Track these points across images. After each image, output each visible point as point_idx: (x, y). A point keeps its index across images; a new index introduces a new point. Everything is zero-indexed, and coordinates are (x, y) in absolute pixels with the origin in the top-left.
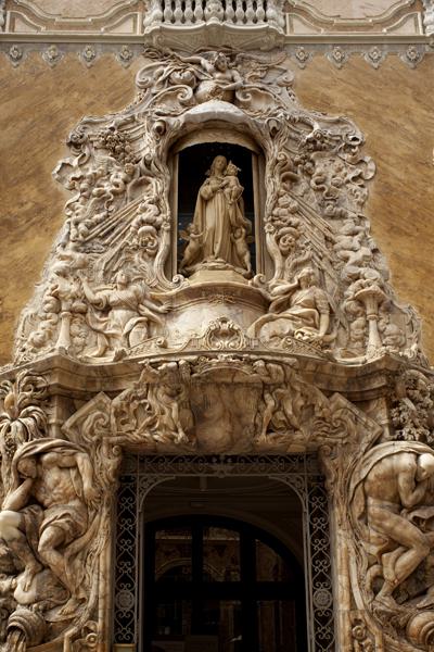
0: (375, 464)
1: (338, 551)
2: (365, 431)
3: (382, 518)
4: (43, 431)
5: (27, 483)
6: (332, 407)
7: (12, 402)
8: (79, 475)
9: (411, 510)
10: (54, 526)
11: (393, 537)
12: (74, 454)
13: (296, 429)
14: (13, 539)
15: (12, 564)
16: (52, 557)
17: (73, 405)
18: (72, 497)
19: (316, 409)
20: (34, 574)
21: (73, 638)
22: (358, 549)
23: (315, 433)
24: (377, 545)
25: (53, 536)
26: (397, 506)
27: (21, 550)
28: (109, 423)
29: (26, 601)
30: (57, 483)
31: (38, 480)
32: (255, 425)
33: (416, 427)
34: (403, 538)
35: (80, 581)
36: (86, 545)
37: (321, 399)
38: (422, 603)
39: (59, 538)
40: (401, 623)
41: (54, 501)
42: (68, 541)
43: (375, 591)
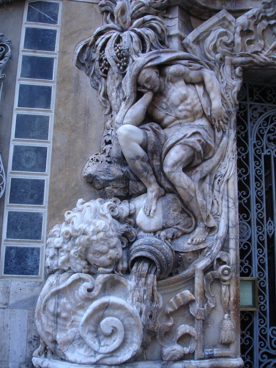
4: (162, 43)
5: (147, 97)
7: (123, 11)
8: (206, 93)
10: (185, 144)
12: (201, 68)
14: (138, 157)
15: (127, 187)
16: (182, 179)
17: (189, 21)
18: (199, 115)
20: (159, 197)
21: (206, 270)
25: (183, 156)
27: (145, 169)
28: (233, 42)
29: (153, 227)
30: (184, 99)
31: (159, 94)
35: (209, 207)
36: (214, 168)
39: (188, 159)
41: (177, 118)
42: (197, 161)
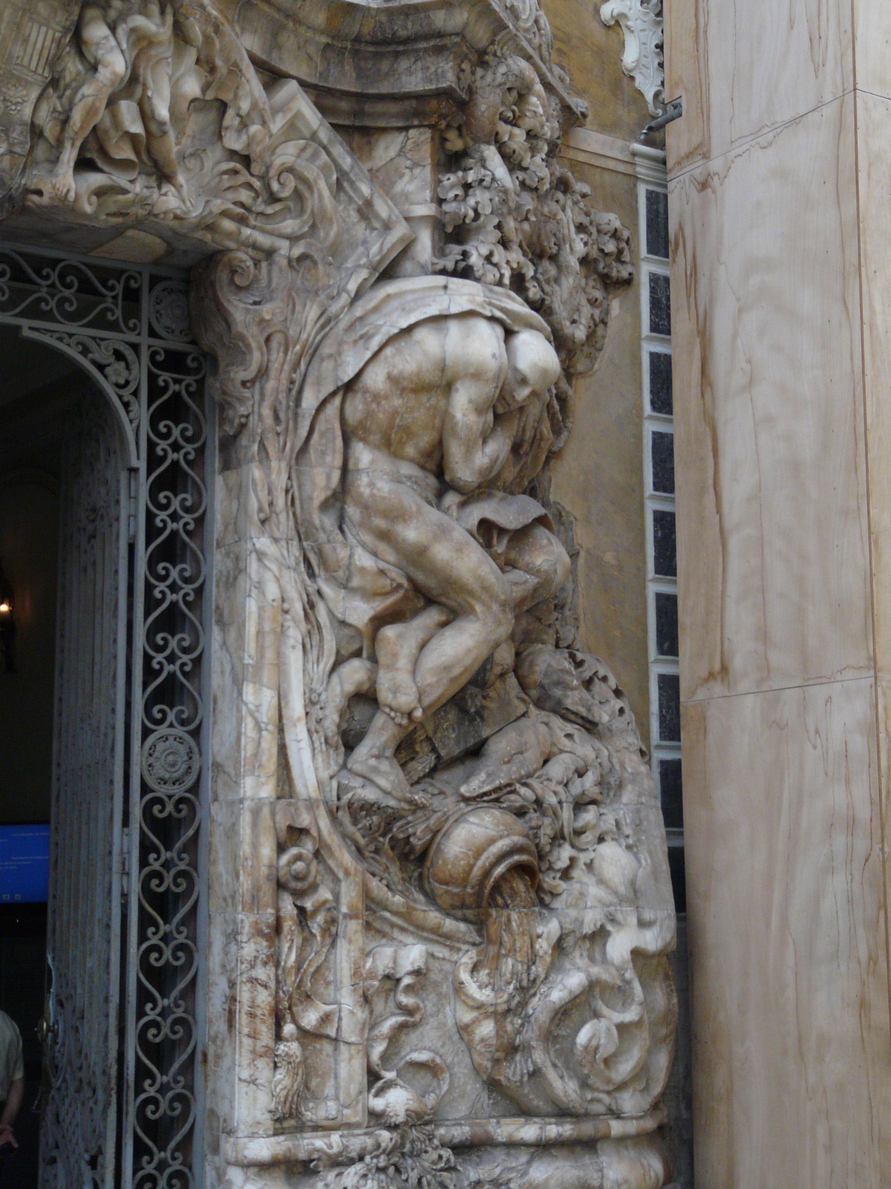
0: (390, 341)
1: (252, 606)
2: (360, 230)
3: (397, 515)
6: (277, 125)
9: (471, 495)
11: (420, 577)
13: (162, 175)
22: (312, 606)
23: (218, 205)
24: (370, 595)
26: (432, 481)
32: (35, 132)
33: (504, 243)
34: (451, 584)
38: (476, 784)
40: (417, 843)
43: (349, 740)
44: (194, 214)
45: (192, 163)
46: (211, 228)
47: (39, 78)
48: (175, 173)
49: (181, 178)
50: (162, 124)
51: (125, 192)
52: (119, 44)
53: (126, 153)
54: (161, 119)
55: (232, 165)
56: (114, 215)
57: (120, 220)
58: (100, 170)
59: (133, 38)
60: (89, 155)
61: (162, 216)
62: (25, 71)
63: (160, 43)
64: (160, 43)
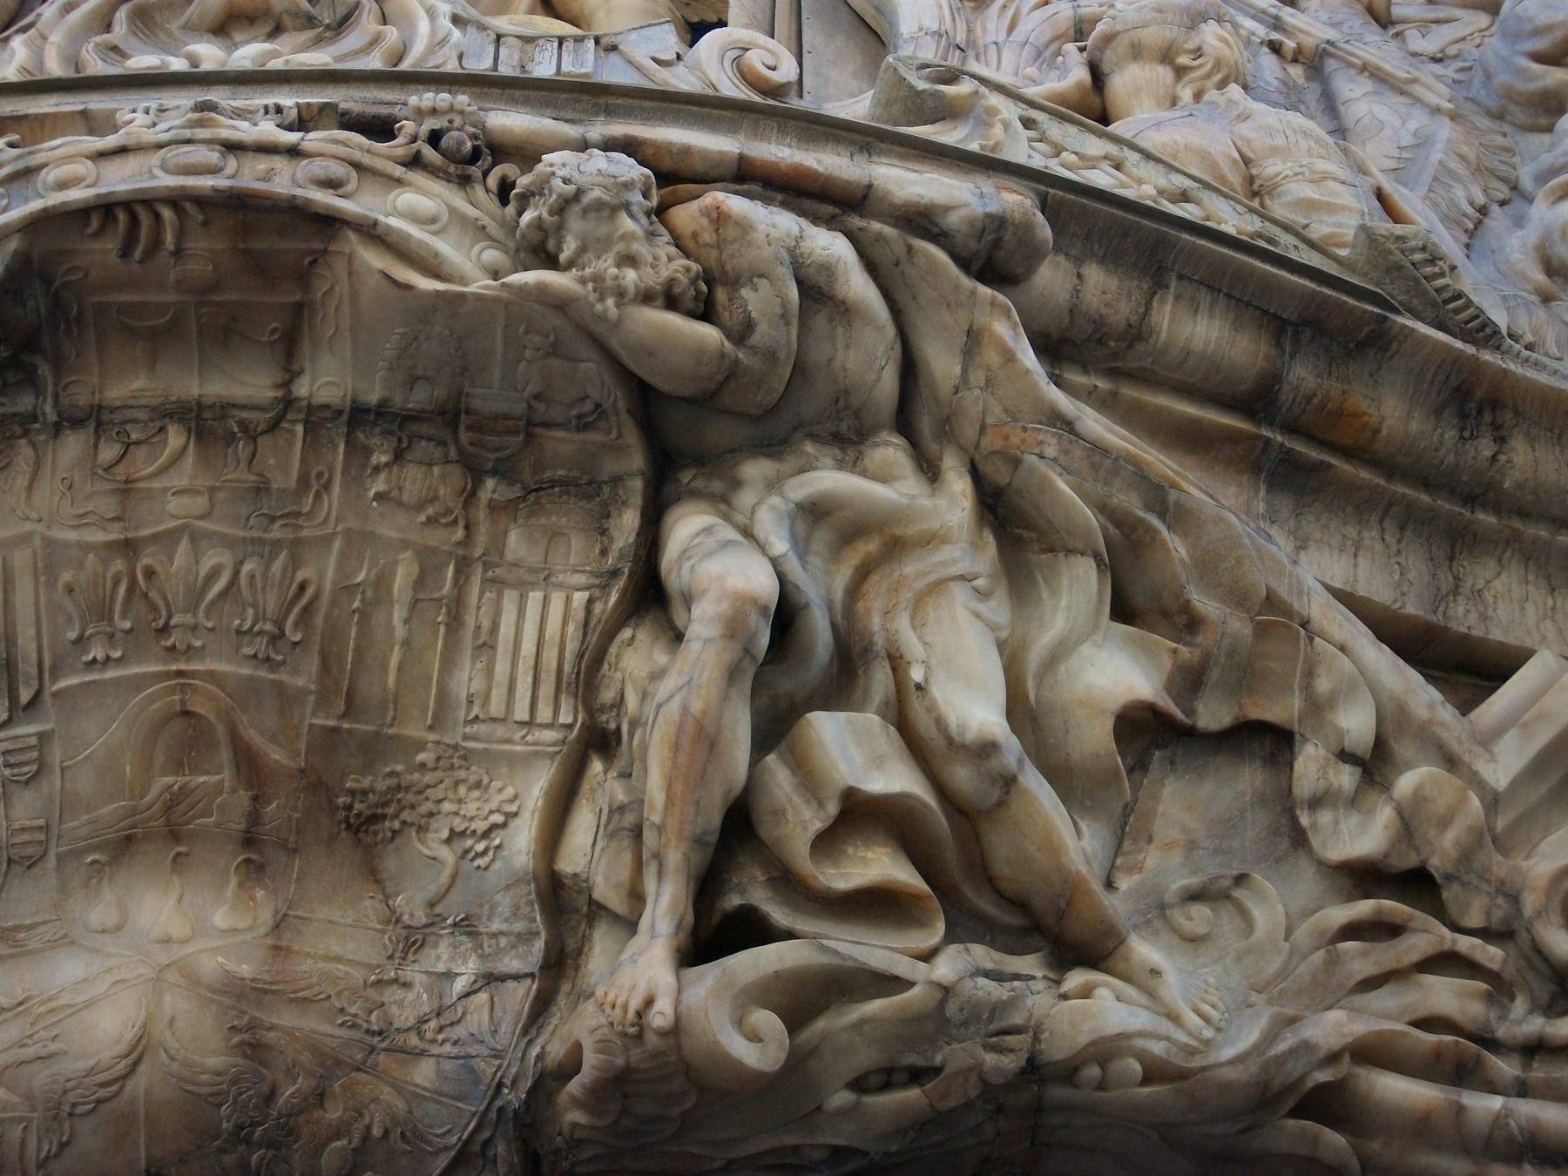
19: (1311, 765)
23: (1333, 1026)
37: (1366, 682)
44: (1228, 1053)
45: (1199, 917)
46: (1328, 1104)
47: (550, 735)
48: (1121, 941)
49: (1144, 950)
50: (986, 749)
51: (890, 983)
52: (762, 547)
53: (877, 865)
54: (970, 736)
55: (1364, 908)
56: (888, 1077)
57: (913, 1094)
58: (789, 935)
59: (823, 537)
60: (734, 901)
61: (1094, 1071)
62: (500, 731)
63: (931, 540)
64: (931, 540)
